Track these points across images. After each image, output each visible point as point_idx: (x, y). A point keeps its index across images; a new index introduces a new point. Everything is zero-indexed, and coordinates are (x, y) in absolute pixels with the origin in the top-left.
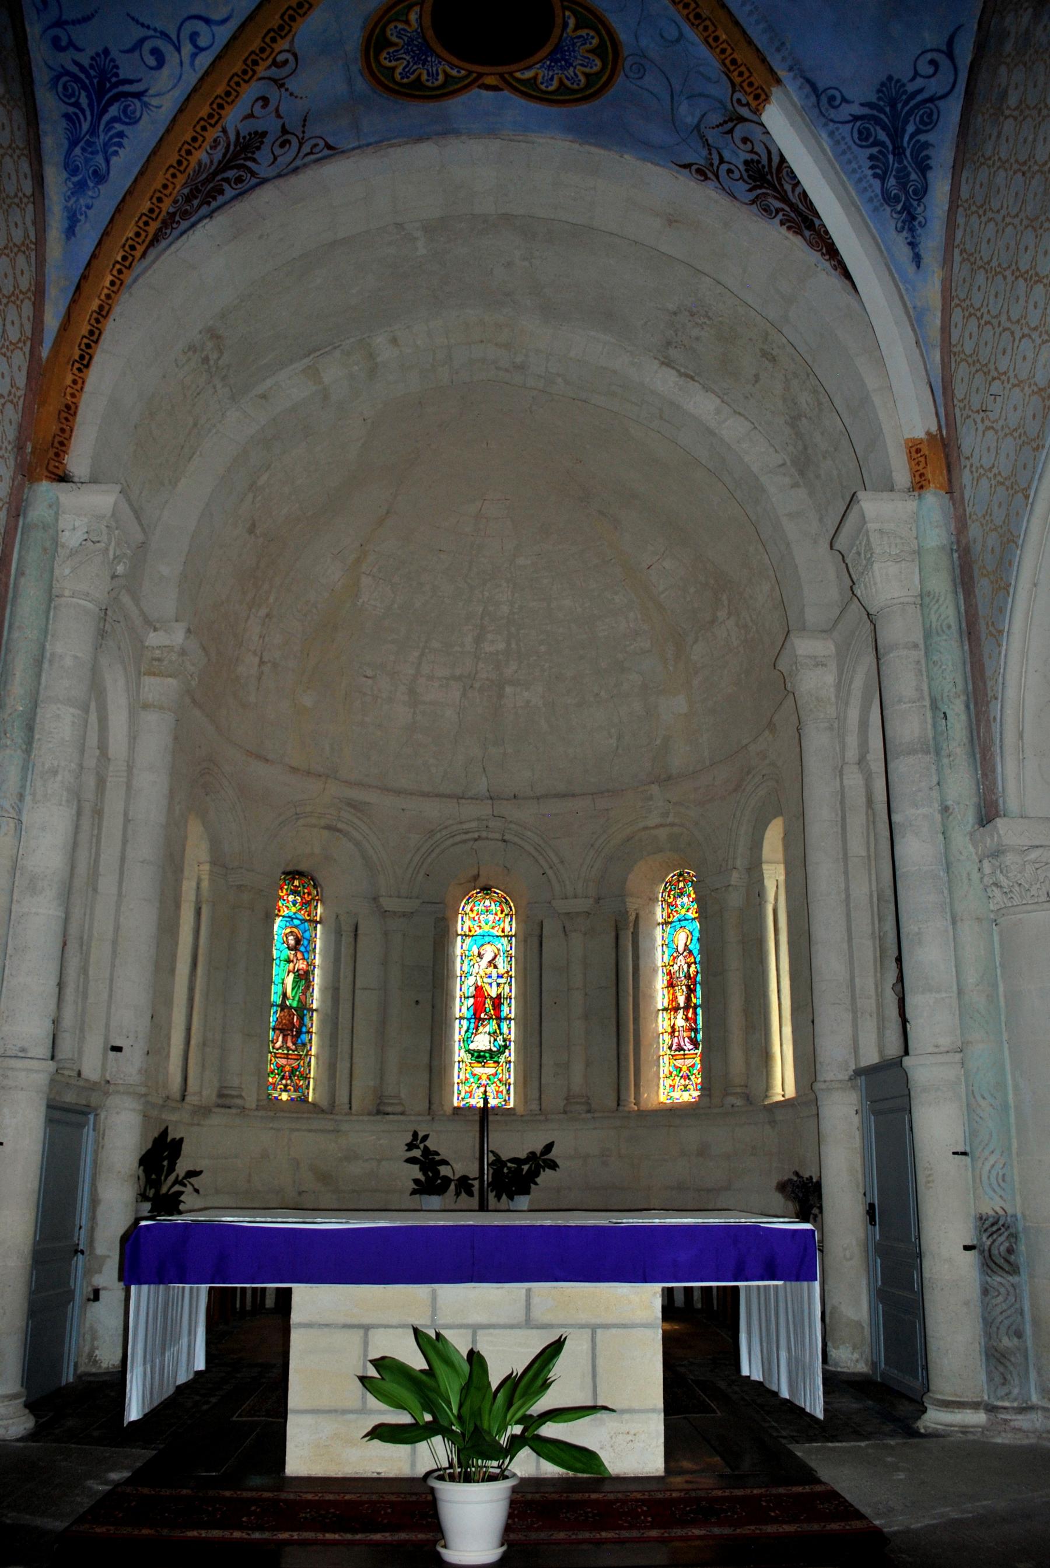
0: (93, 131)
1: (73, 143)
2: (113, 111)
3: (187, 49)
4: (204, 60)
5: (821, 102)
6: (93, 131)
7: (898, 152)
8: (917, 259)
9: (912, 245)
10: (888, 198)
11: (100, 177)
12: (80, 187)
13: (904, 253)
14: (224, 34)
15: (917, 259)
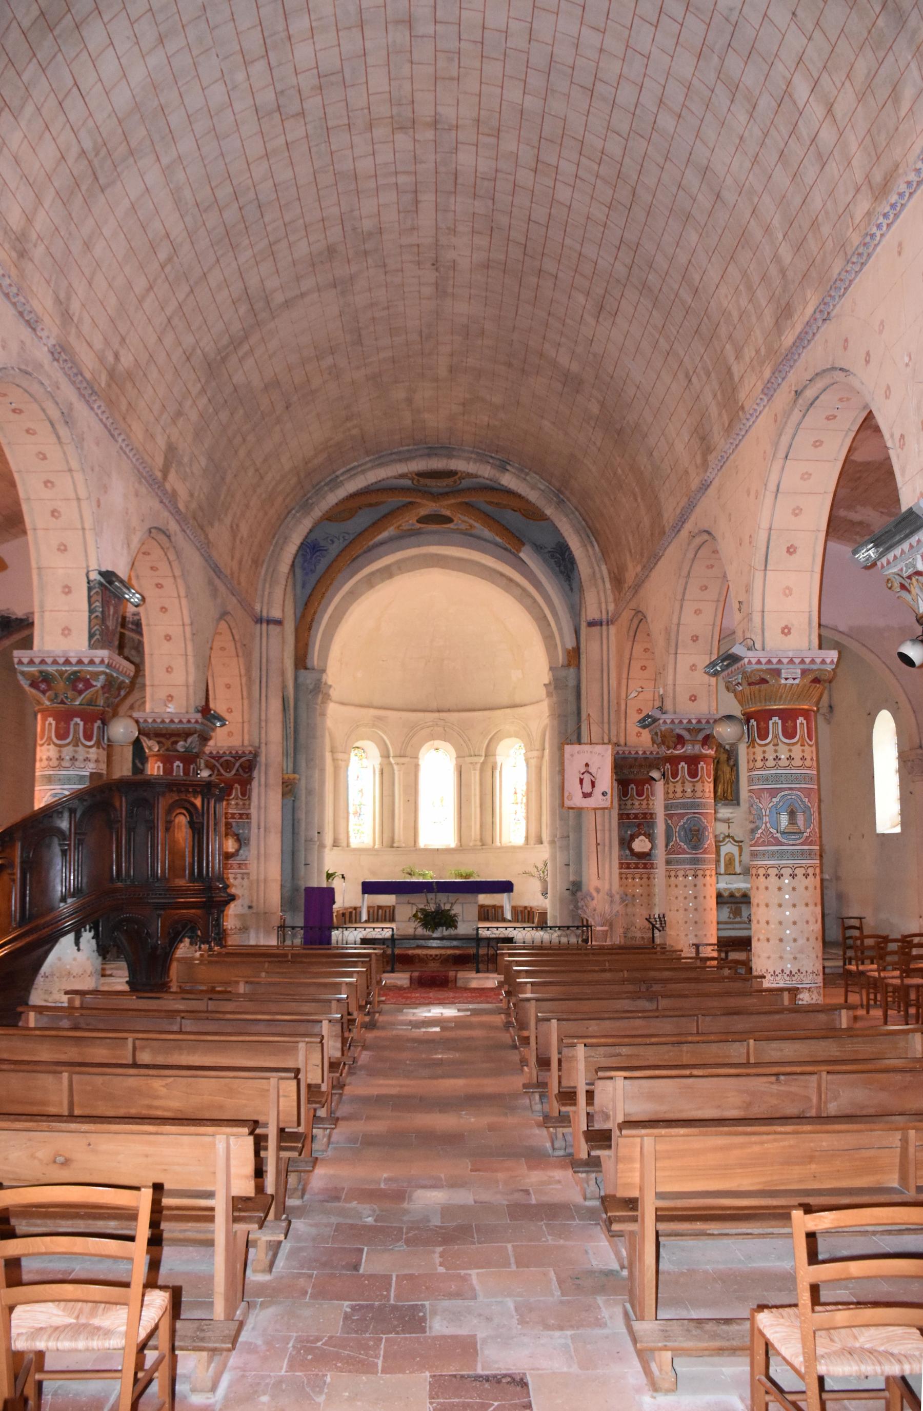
0: (311, 558)
1: (305, 561)
2: (318, 554)
3: (342, 540)
4: (347, 542)
5: (538, 548)
6: (311, 558)
7: (564, 560)
8: (572, 589)
9: (570, 585)
10: (561, 572)
11: (313, 571)
12: (307, 574)
13: (567, 588)
14: (352, 537)
15: (572, 589)
